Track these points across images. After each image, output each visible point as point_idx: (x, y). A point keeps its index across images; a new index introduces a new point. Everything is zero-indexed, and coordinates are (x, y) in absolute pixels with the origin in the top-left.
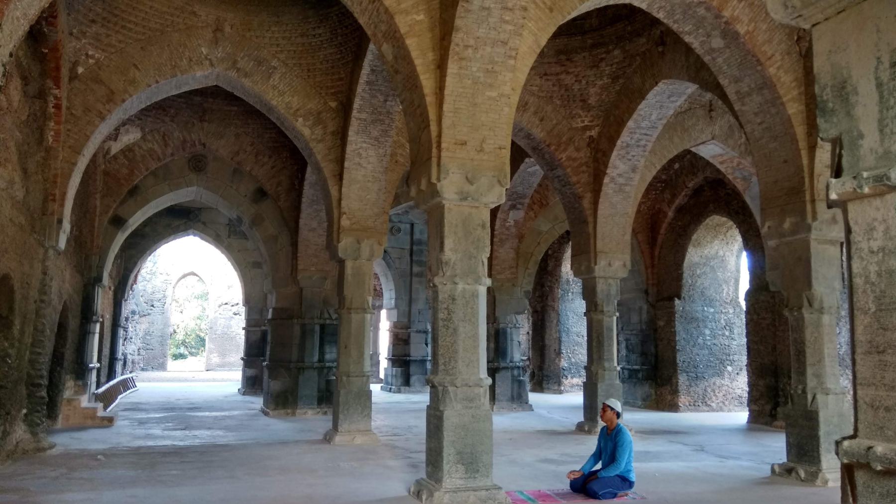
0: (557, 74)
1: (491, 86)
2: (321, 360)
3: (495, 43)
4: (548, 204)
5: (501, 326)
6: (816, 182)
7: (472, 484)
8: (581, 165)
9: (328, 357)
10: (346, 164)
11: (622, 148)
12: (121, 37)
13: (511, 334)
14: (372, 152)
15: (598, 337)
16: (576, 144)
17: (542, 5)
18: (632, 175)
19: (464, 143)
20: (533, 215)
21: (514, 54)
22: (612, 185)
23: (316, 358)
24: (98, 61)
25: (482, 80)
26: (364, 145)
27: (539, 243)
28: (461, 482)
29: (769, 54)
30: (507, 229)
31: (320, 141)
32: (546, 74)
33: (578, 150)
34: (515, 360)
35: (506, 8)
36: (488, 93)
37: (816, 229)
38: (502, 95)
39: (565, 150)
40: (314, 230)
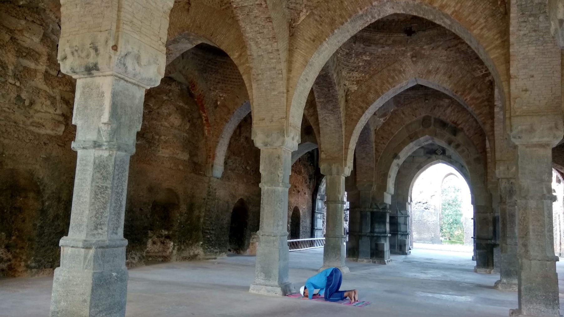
0: (456, 45)
1: (274, 89)
2: (372, 231)
3: (270, 70)
6: (512, 103)
7: (267, 283)
8: (483, 101)
9: (377, 230)
10: (320, 126)
12: (231, 86)
14: (331, 118)
15: (503, 221)
16: (479, 88)
17: (309, 40)
19: (264, 119)
21: (280, 72)
23: (369, 230)
24: (224, 97)
25: (269, 88)
26: (327, 115)
28: (263, 281)
29: (474, 20)
31: (312, 116)
32: (449, 47)
33: (480, 91)
35: (269, 53)
36: (273, 93)
37: (514, 138)
38: (279, 93)
39: (469, 93)
40: (364, 158)
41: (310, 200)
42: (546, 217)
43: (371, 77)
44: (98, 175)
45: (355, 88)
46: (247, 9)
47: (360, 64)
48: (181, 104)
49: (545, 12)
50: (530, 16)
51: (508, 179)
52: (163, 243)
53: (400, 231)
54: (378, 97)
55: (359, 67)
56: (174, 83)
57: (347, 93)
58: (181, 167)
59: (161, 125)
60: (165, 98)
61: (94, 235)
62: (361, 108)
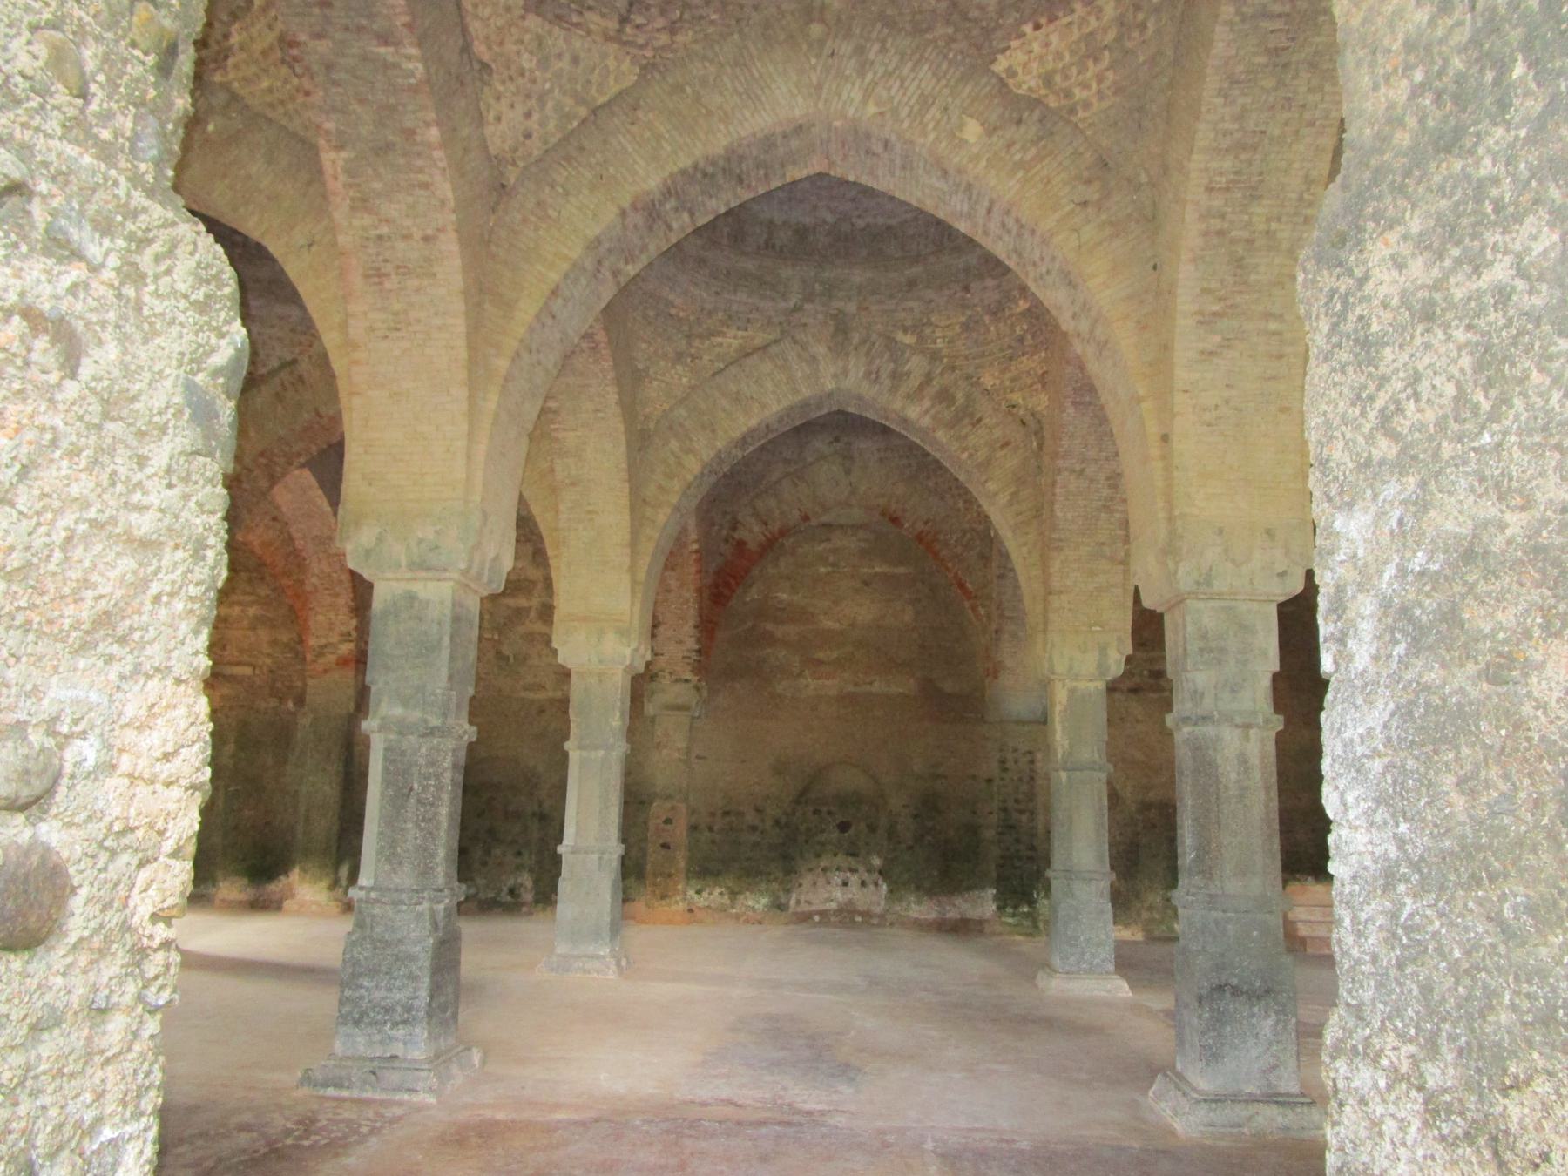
48: (878, 569)
55: (1021, 340)
60: (823, 570)
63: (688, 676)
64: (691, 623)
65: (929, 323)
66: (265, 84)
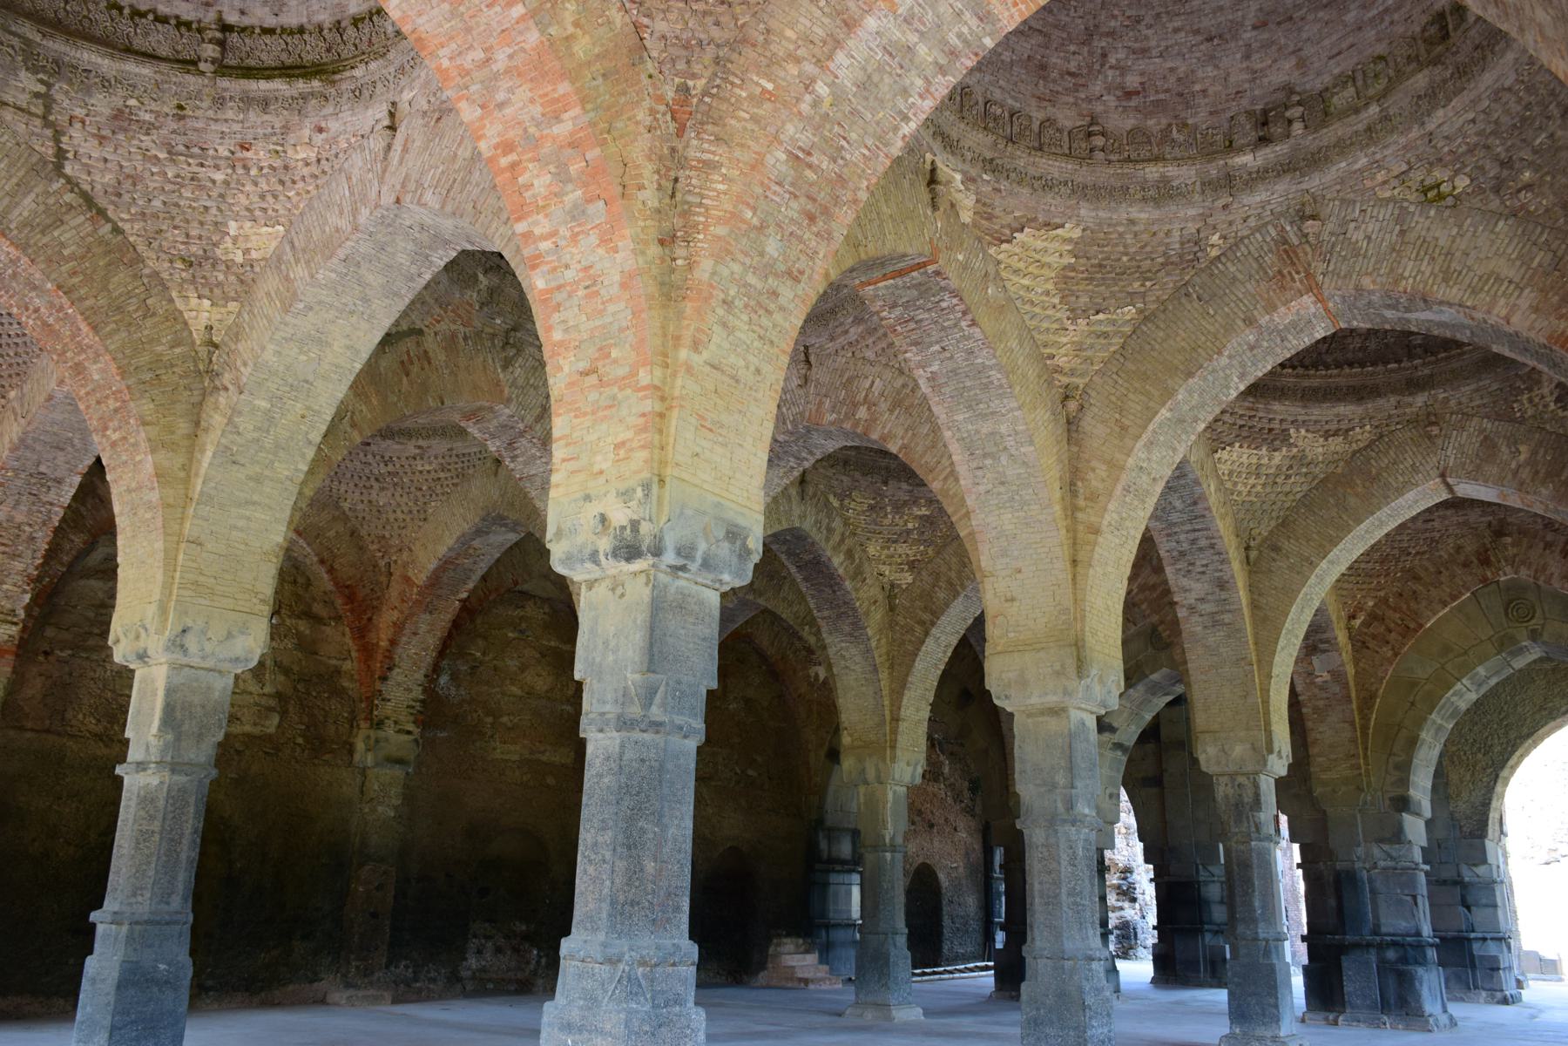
4: (1421, 626)
5: (1339, 866)
11: (1176, 560)
13: (1371, 881)
14: (853, 651)
18: (1224, 595)
20: (1390, 654)
22: (1195, 618)
27: (1413, 704)
30: (1321, 688)
34: (1384, 930)
41: (978, 846)
42: (1064, 863)
43: (938, 553)
44: (142, 813)
45: (908, 578)
46: (538, 482)
47: (910, 526)
49: (1005, 448)
50: (985, 456)
51: (1232, 776)
52: (516, 950)
53: (1211, 923)
54: (955, 597)
55: (909, 532)
56: (531, 603)
57: (891, 591)
58: (550, 781)
59: (504, 694)
61: (130, 904)
62: (922, 623)
63: (411, 727)
64: (423, 672)
65: (850, 496)
66: (1026, 282)
